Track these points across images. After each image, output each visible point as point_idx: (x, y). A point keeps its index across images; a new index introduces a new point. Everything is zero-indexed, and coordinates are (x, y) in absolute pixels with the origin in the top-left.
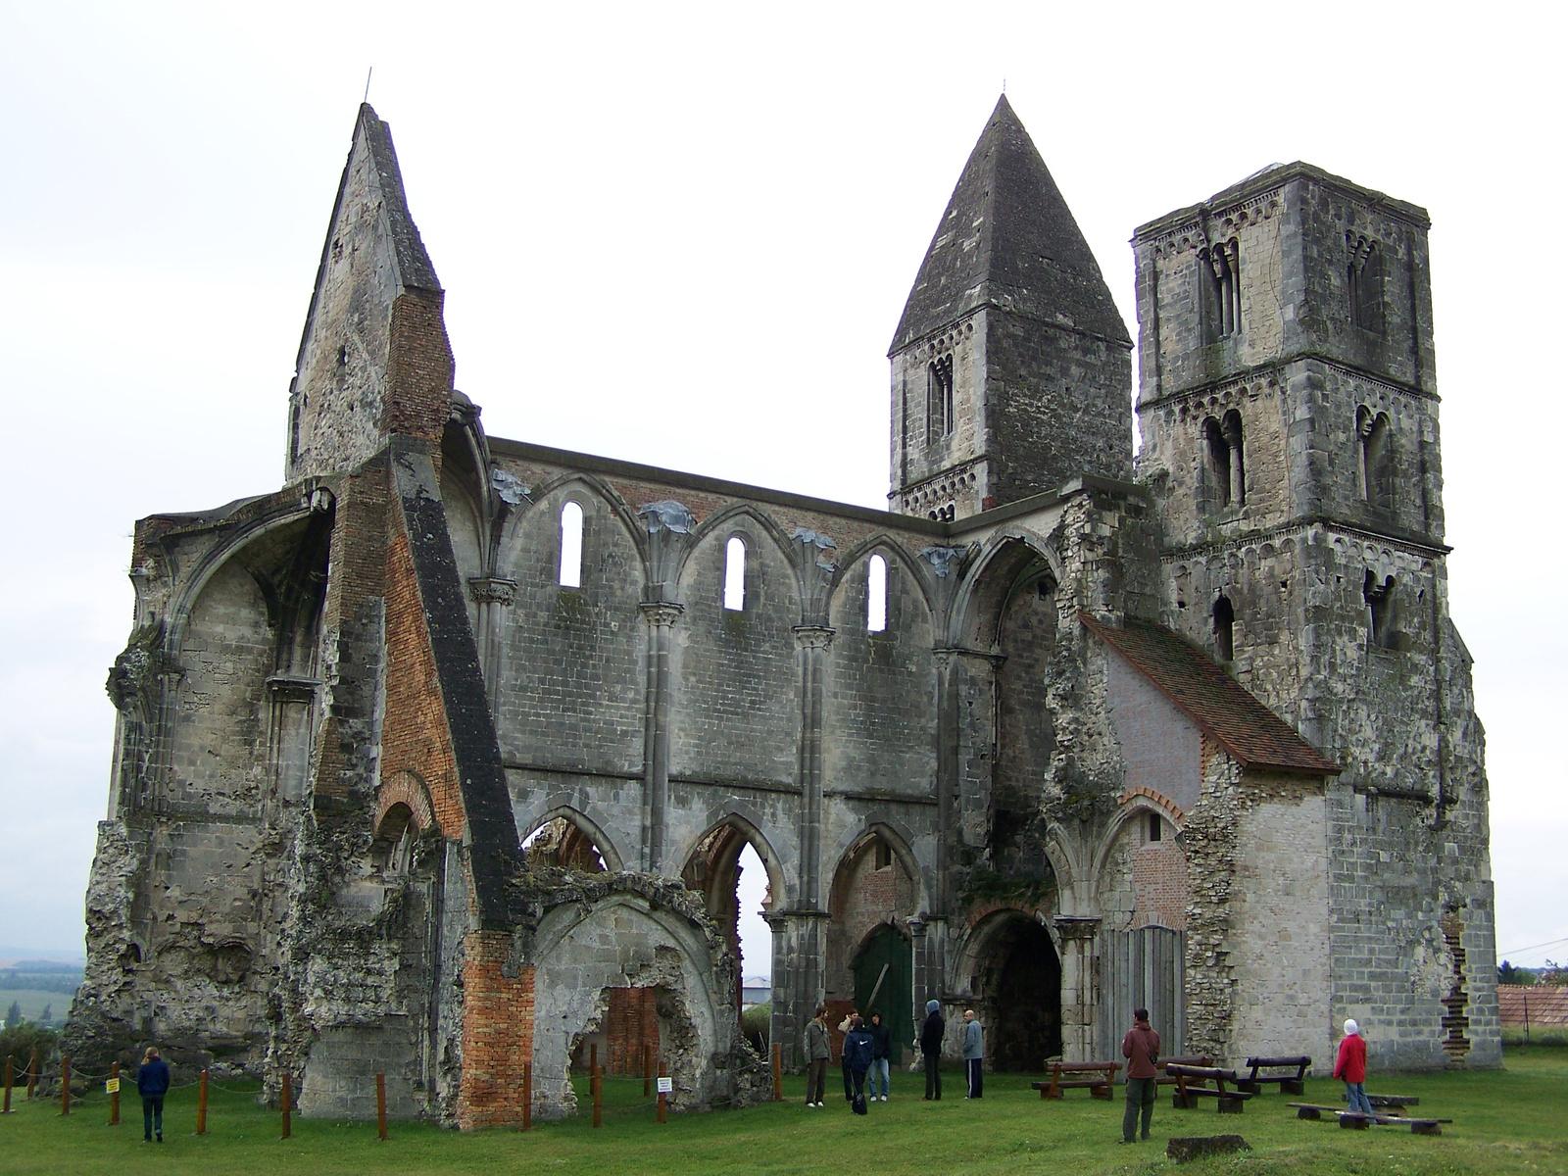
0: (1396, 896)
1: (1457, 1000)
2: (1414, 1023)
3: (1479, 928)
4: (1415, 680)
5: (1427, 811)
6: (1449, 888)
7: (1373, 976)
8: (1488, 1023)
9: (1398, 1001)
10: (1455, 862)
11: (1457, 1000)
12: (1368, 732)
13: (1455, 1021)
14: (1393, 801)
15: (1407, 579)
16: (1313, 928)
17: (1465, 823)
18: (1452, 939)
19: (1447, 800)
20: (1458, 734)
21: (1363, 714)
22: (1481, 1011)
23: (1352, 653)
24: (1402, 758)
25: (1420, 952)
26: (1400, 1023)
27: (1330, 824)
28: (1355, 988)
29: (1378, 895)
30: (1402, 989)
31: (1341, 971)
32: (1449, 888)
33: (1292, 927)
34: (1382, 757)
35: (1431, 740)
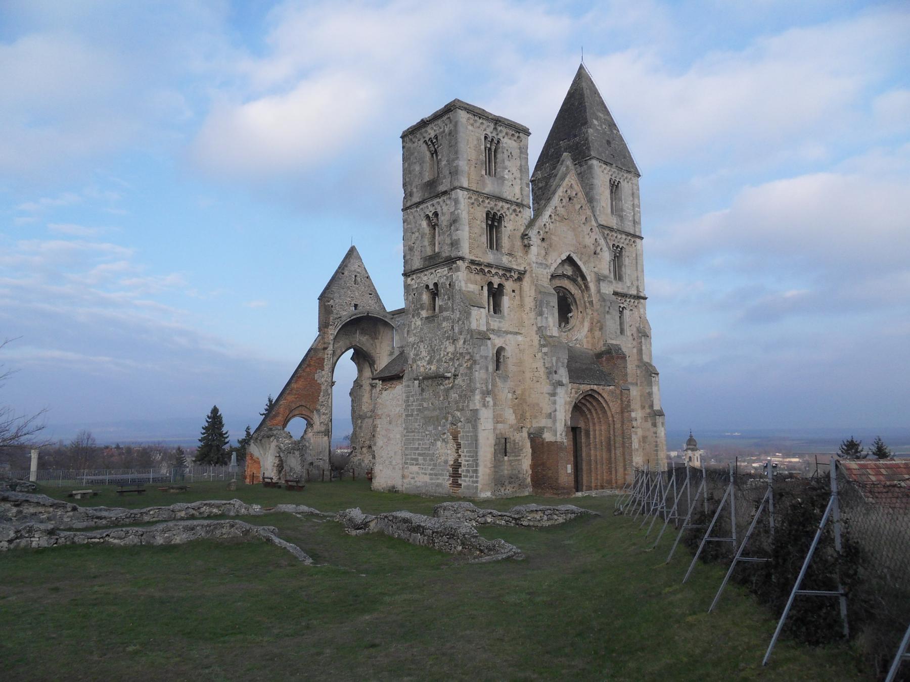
0: (428, 421)
1: (457, 466)
2: (436, 475)
3: (469, 432)
4: (445, 324)
5: (447, 382)
6: (453, 416)
7: (419, 455)
8: (471, 477)
9: (430, 465)
10: (457, 402)
11: (457, 466)
12: (424, 354)
13: (455, 475)
14: (430, 381)
15: (442, 280)
16: (398, 436)
17: (461, 383)
18: (455, 438)
19: (455, 376)
20: (461, 342)
21: (422, 347)
22: (468, 471)
23: (419, 323)
24: (438, 361)
25: (439, 443)
26: (430, 474)
27: (404, 395)
28: (412, 459)
29: (422, 421)
30: (432, 460)
31: (407, 452)
32: (453, 416)
33: (392, 436)
34: (430, 362)
35: (451, 349)
